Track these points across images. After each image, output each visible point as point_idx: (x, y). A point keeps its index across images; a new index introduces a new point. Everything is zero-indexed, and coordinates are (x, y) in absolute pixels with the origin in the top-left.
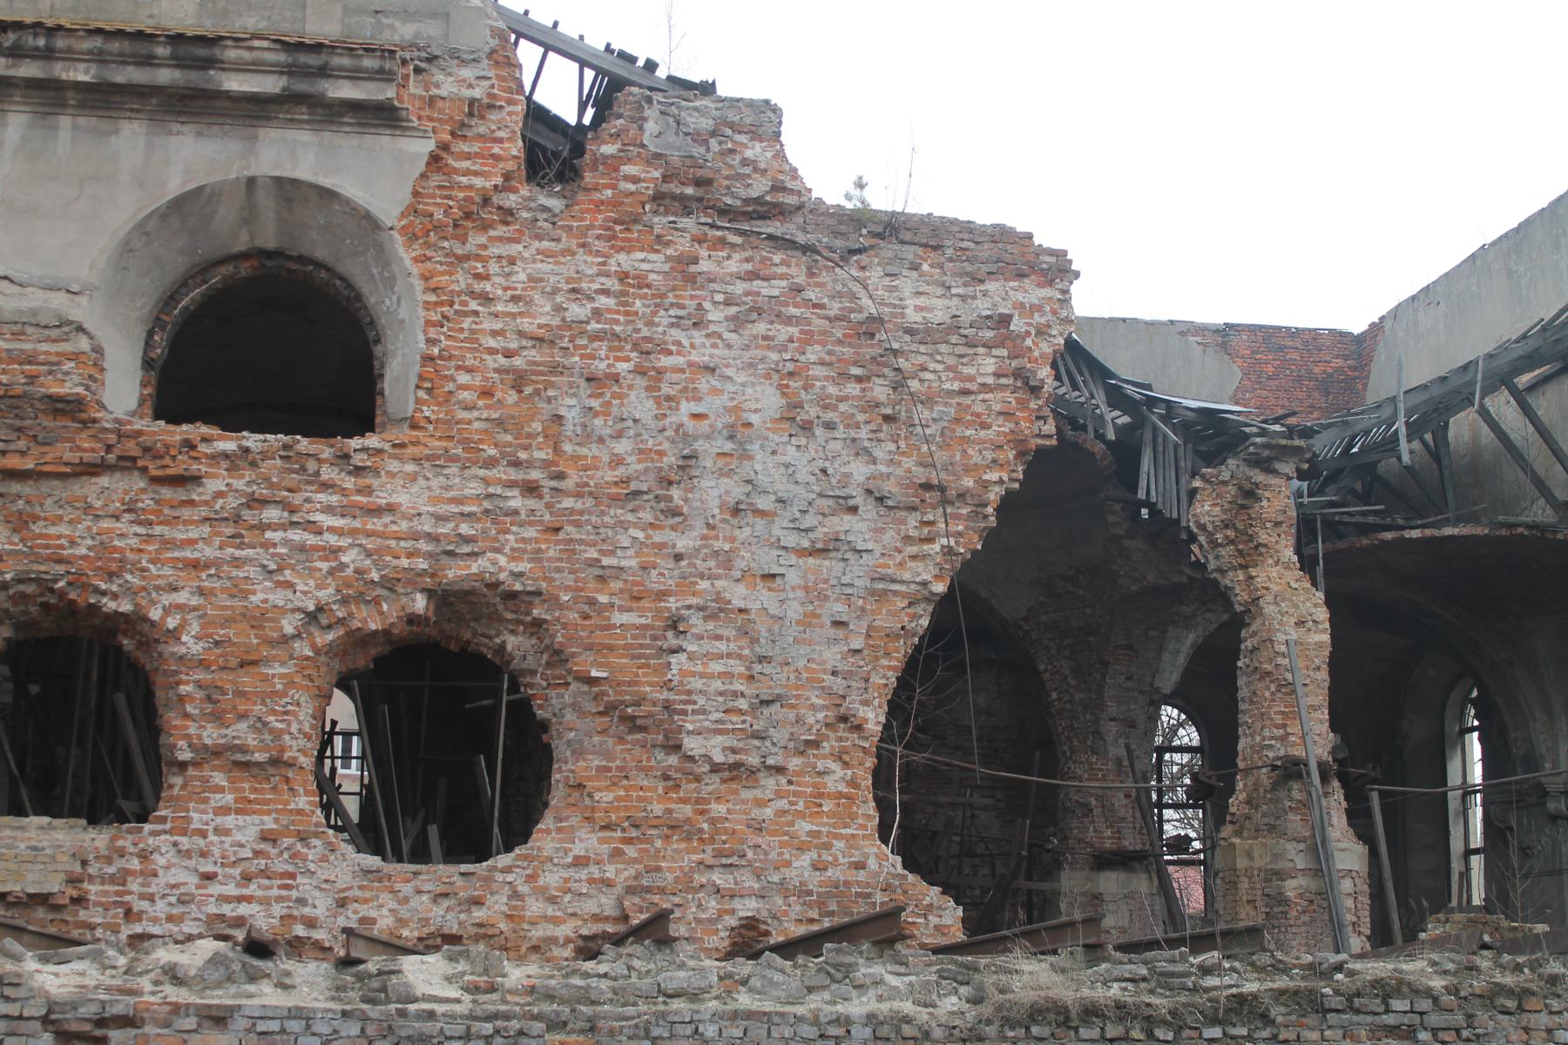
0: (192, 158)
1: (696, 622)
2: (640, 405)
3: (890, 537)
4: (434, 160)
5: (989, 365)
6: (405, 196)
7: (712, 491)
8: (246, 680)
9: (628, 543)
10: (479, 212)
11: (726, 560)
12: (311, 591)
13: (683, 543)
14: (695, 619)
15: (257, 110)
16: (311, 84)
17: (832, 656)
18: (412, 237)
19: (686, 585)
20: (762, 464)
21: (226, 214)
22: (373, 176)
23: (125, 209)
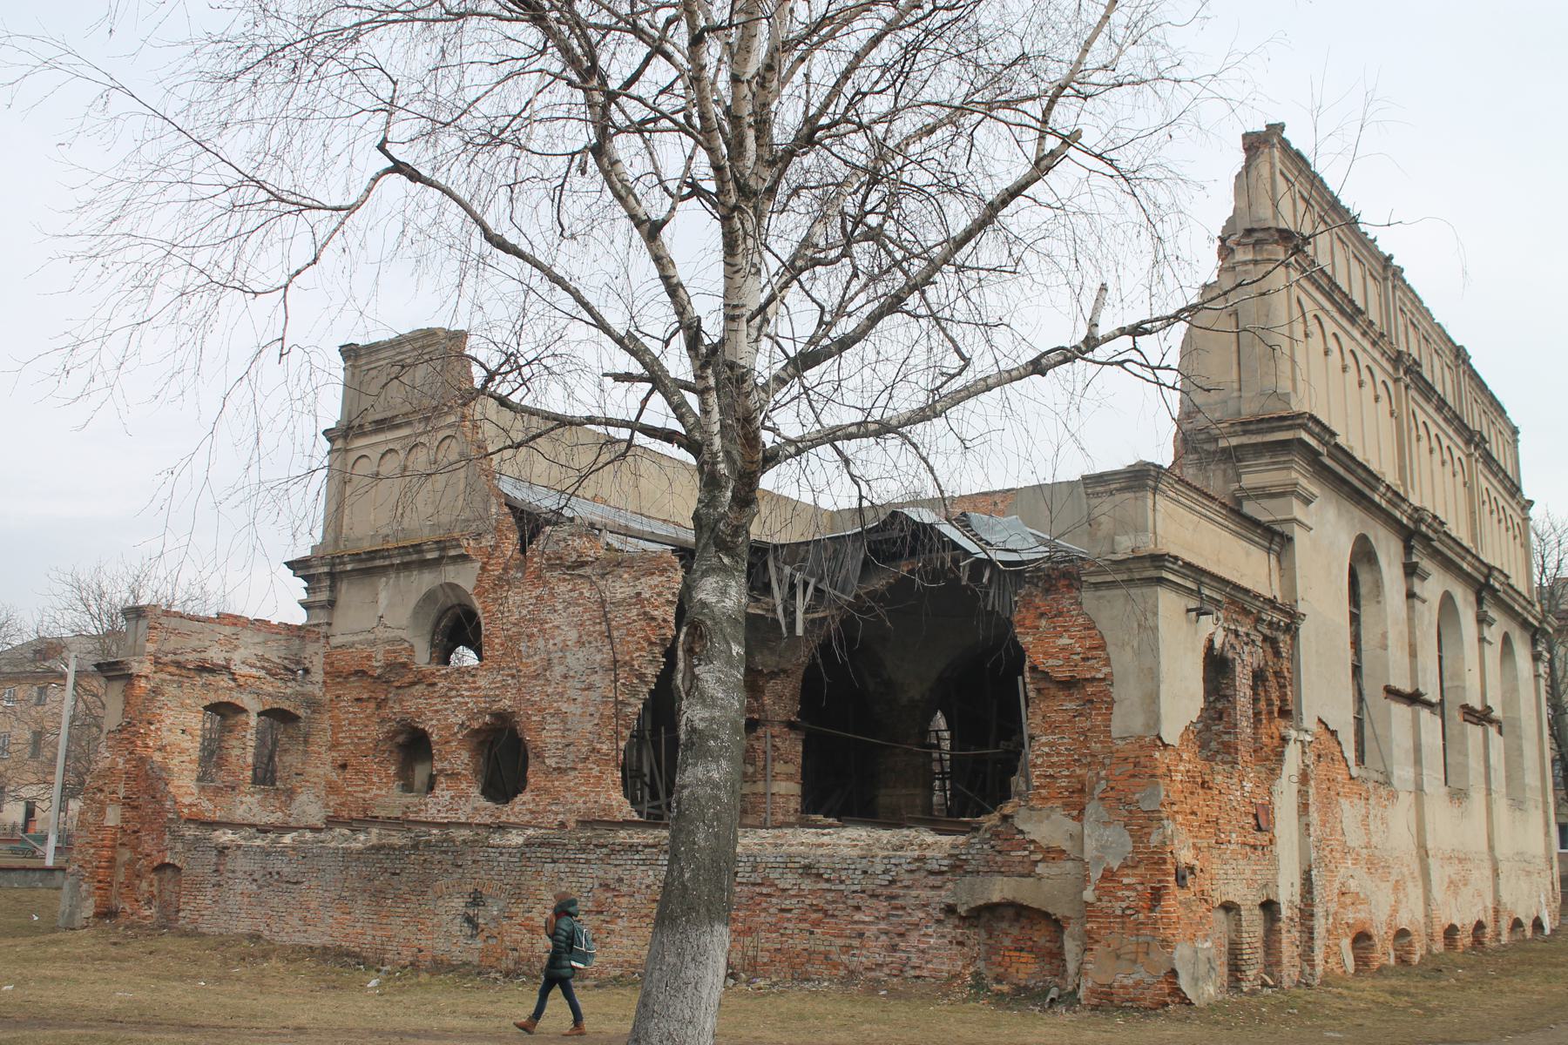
0: (426, 581)
1: (549, 719)
2: (541, 643)
3: (607, 681)
4: (483, 568)
5: (635, 612)
6: (473, 582)
7: (558, 670)
8: (447, 747)
9: (536, 693)
10: (502, 582)
11: (561, 695)
12: (461, 717)
13: (550, 690)
14: (549, 719)
15: (437, 562)
16: (445, 552)
17: (589, 727)
18: (479, 595)
19: (551, 706)
20: (570, 660)
21: (440, 594)
22: (465, 578)
23: (413, 599)
